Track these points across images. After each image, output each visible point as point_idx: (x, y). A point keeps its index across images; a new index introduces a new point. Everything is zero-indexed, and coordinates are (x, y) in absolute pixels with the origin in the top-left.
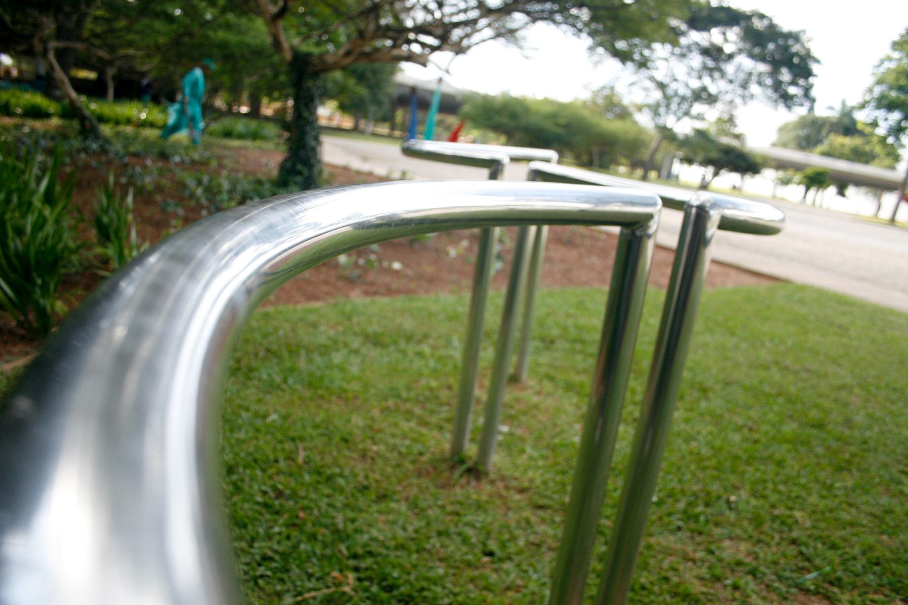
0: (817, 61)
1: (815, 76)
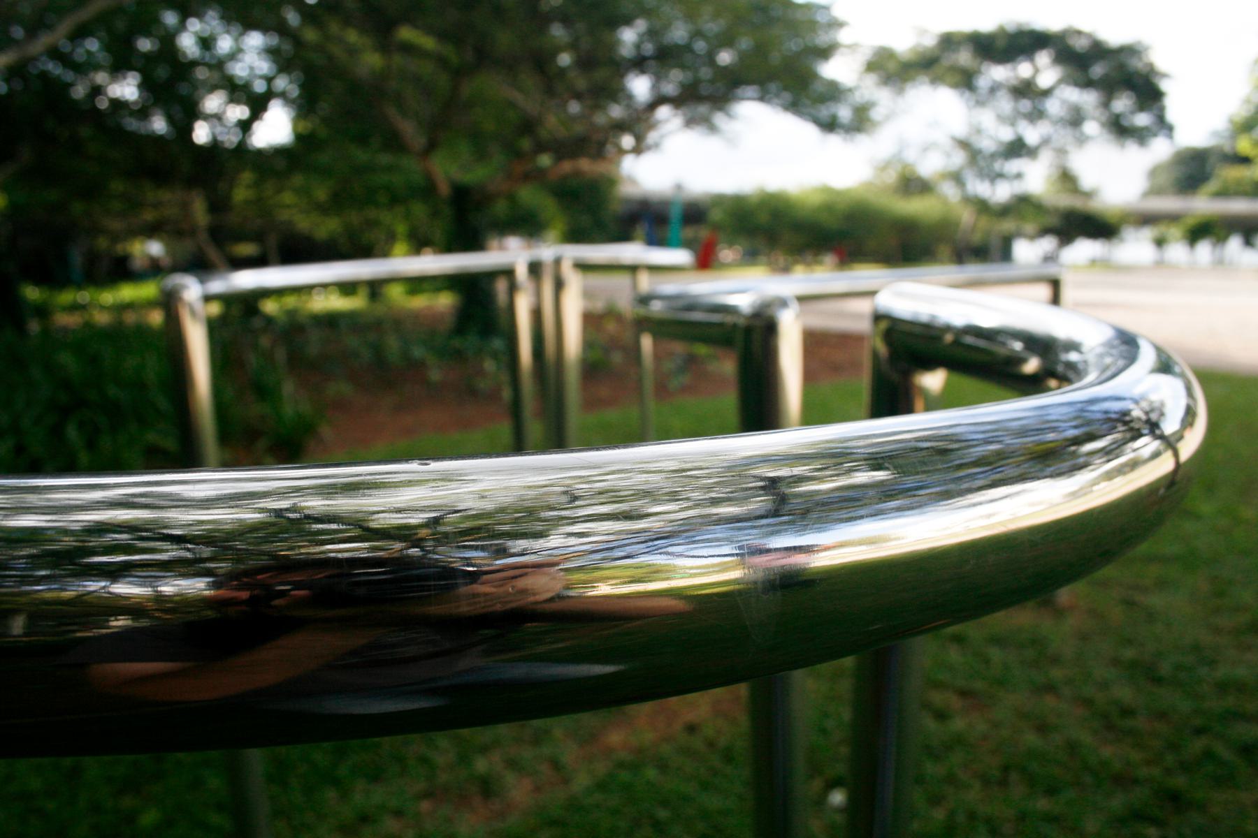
0: (1164, 76)
1: (850, 90)
